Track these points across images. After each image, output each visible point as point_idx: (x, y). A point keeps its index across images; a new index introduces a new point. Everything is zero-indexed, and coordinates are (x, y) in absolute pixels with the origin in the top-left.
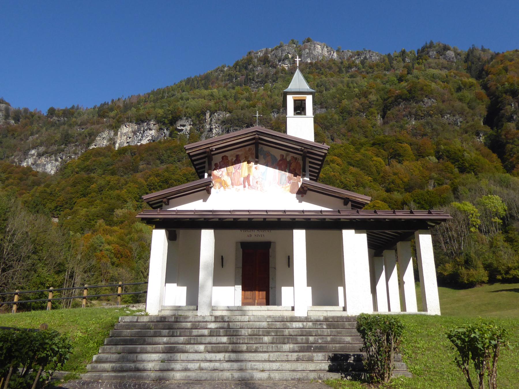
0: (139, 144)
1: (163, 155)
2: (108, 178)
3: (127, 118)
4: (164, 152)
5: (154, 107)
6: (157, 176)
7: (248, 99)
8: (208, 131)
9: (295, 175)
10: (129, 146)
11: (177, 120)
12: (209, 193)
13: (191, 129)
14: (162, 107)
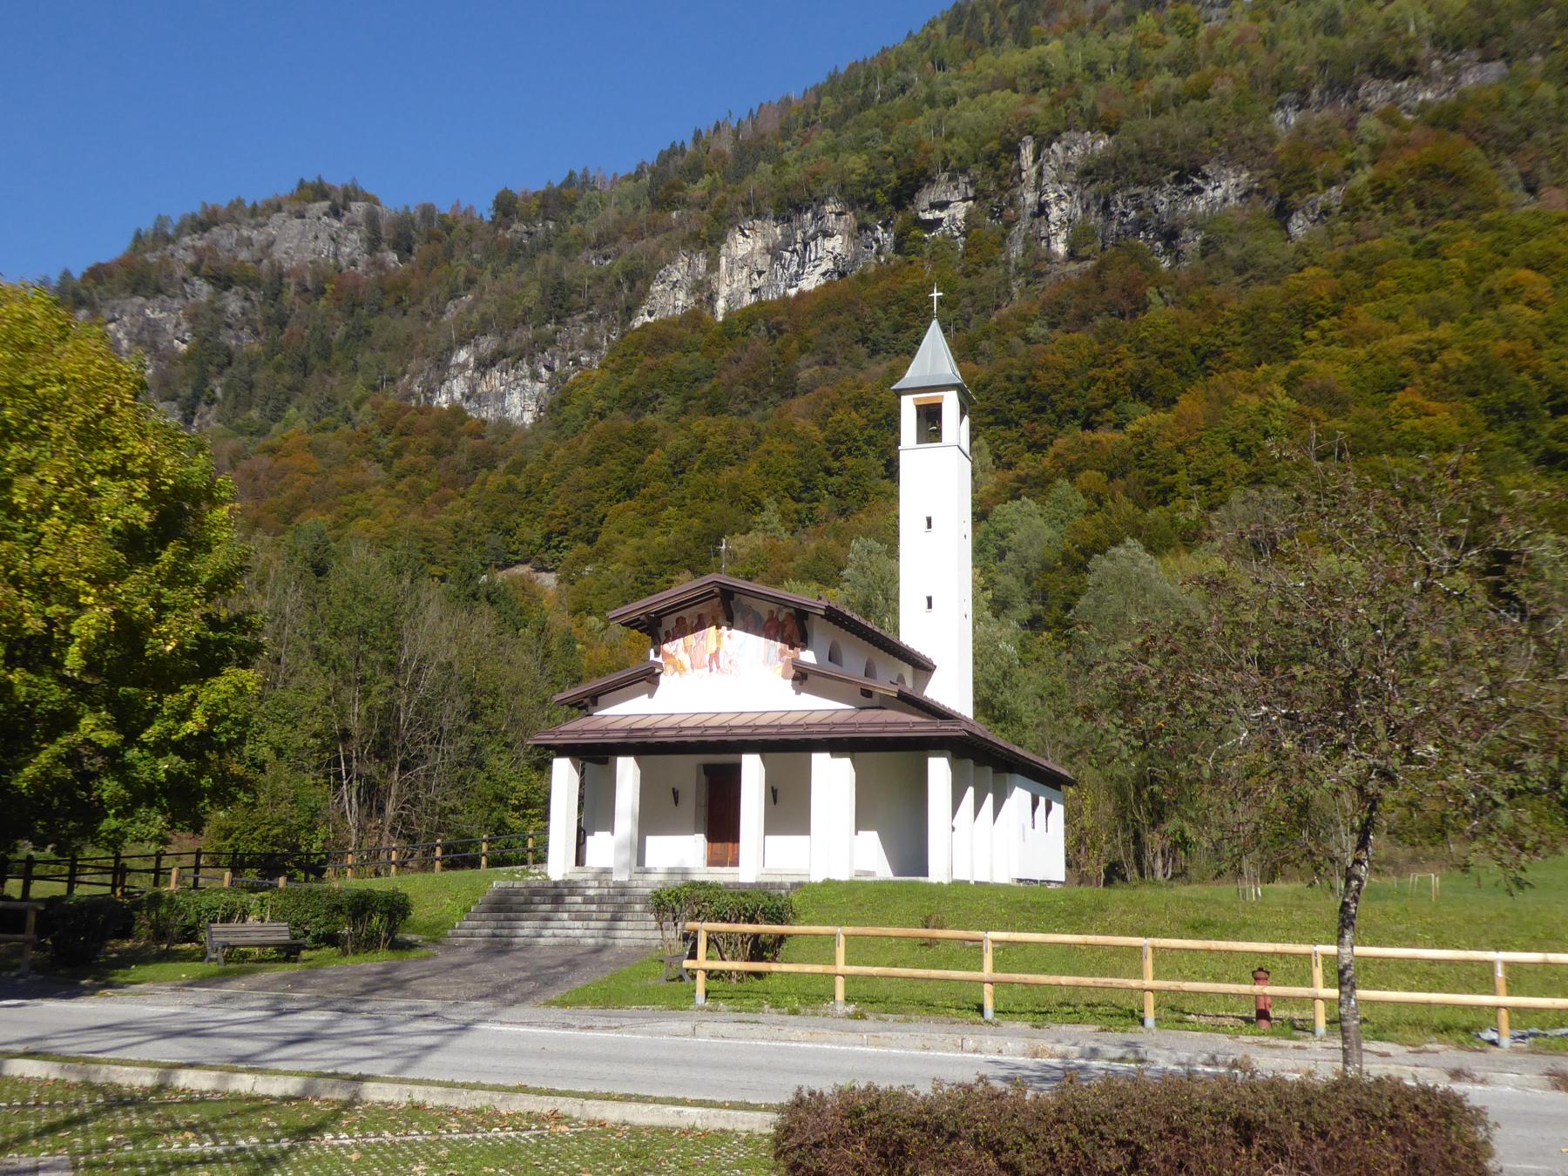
0: (793, 292)
1: (876, 324)
2: (700, 424)
3: (746, 204)
4: (880, 314)
5: (833, 149)
6: (856, 407)
7: (1181, 66)
8: (1035, 215)
9: (792, 647)
10: (759, 303)
11: (918, 188)
12: (656, 683)
13: (969, 210)
14: (860, 146)
